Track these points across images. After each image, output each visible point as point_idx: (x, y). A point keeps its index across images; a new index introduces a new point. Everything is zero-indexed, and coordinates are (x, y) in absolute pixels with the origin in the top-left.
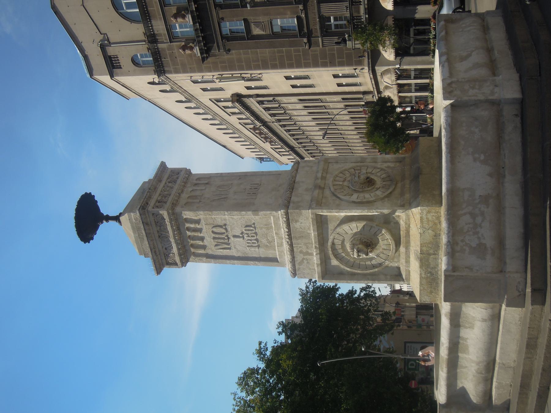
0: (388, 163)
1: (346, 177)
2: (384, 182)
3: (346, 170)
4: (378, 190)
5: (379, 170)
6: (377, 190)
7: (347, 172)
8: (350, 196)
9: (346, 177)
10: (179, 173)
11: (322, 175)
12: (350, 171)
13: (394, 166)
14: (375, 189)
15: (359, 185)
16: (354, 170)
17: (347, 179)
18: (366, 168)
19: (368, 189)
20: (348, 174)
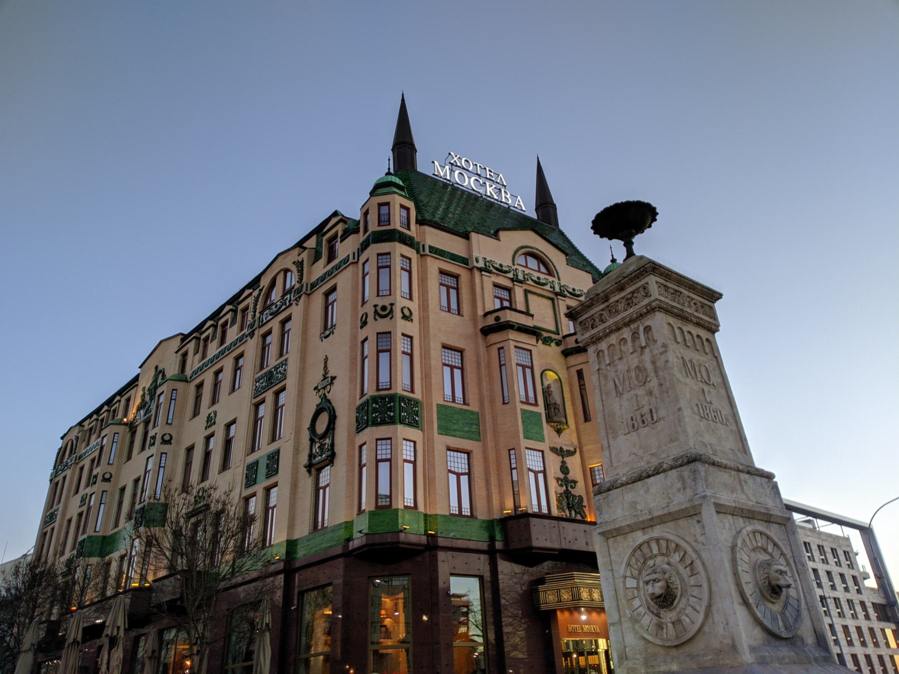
8: (630, 575)
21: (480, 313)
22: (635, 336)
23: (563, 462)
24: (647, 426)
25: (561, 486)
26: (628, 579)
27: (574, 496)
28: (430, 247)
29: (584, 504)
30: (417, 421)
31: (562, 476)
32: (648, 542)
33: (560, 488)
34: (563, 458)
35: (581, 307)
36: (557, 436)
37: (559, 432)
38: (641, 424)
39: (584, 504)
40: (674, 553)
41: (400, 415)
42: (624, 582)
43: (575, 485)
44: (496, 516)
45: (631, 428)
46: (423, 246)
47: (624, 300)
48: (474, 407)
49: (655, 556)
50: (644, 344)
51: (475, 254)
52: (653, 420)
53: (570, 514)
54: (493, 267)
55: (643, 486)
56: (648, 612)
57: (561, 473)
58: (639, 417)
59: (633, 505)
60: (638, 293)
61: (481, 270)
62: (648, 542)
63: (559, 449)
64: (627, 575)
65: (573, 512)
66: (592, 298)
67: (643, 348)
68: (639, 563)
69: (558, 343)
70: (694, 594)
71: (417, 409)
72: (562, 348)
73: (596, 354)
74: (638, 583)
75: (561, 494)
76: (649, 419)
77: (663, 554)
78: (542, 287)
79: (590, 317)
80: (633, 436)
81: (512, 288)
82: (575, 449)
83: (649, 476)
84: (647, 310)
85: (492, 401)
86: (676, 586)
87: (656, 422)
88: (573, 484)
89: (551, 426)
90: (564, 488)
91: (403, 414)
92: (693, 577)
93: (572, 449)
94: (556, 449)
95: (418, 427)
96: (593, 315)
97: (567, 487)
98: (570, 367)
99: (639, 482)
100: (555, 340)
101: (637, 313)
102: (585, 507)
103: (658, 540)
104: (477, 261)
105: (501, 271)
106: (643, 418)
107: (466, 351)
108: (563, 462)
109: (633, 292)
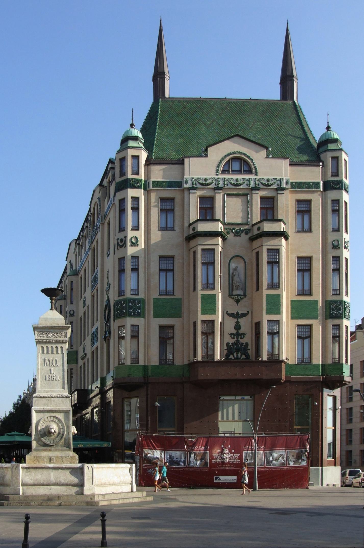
21: (186, 225)
23: (238, 322)
25: (234, 338)
27: (242, 344)
28: (153, 182)
29: (248, 348)
30: (139, 313)
31: (234, 332)
33: (233, 340)
34: (237, 319)
36: (236, 304)
37: (238, 301)
39: (248, 348)
41: (129, 310)
43: (244, 336)
44: (186, 362)
46: (149, 182)
48: (178, 295)
51: (186, 177)
53: (237, 355)
54: (199, 183)
57: (234, 330)
61: (189, 189)
63: (235, 313)
65: (239, 354)
69: (247, 233)
71: (140, 305)
72: (250, 235)
75: (232, 343)
78: (240, 187)
81: (214, 196)
82: (248, 312)
85: (189, 290)
88: (242, 336)
89: (233, 298)
90: (236, 339)
91: (130, 310)
93: (246, 312)
94: (233, 314)
95: (140, 316)
97: (237, 339)
98: (253, 250)
100: (245, 230)
102: (249, 349)
104: (186, 183)
105: (205, 185)
107: (176, 256)
108: (238, 322)
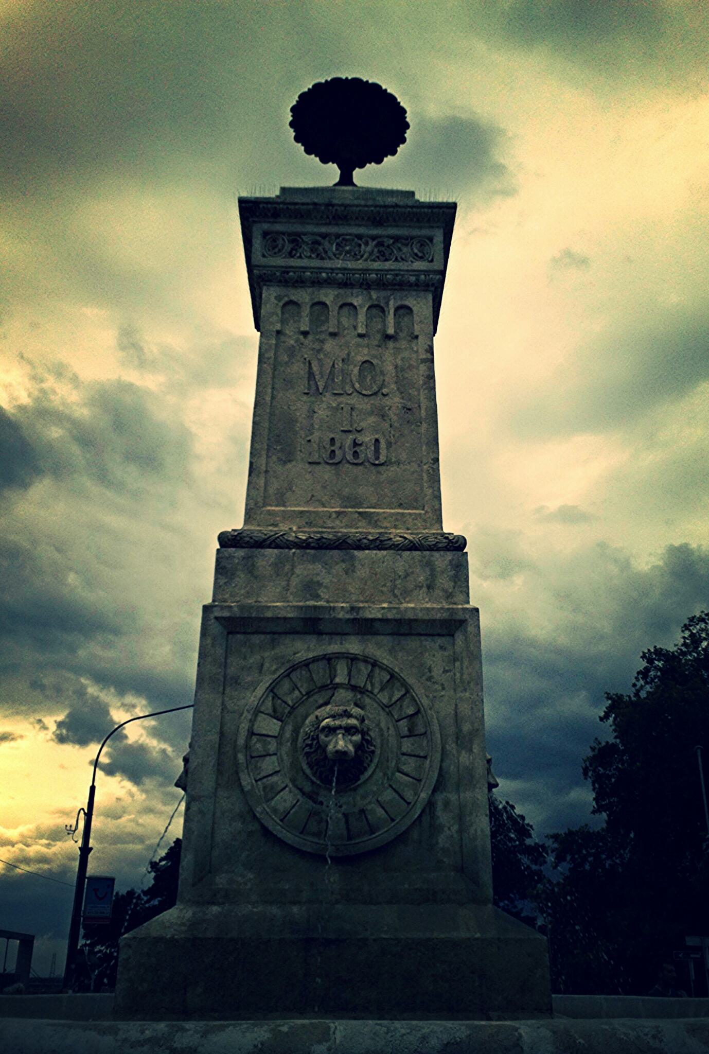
0: (455, 828)
1: (372, 693)
2: (346, 816)
3: (407, 692)
4: (299, 797)
5: (409, 795)
6: (304, 793)
7: (397, 695)
8: (270, 711)
9: (372, 693)
10: (421, 258)
11: (373, 620)
12: (407, 701)
13: (441, 845)
14: (308, 788)
15: (312, 734)
16: (412, 716)
17: (365, 696)
18: (422, 754)
19: (305, 767)
20: (390, 699)
22: (378, 309)
24: (361, 464)
26: (261, 717)
32: (329, 659)
35: (311, 207)
38: (350, 457)
40: (382, 690)
42: (252, 721)
45: (326, 455)
47: (374, 243)
49: (337, 686)
50: (391, 331)
52: (377, 458)
55: (343, 561)
56: (291, 785)
58: (348, 443)
59: (310, 588)
60: (407, 245)
62: (329, 660)
64: (263, 709)
66: (315, 204)
67: (388, 337)
68: (297, 692)
70: (405, 768)
73: (281, 304)
74: (282, 729)
76: (370, 455)
77: (354, 688)
79: (289, 235)
80: (326, 473)
83: (359, 546)
84: (417, 280)
86: (373, 748)
87: (382, 464)
92: (411, 739)
96: (299, 234)
99: (335, 552)
101: (397, 275)
103: (353, 659)
106: (358, 449)
109: (397, 239)
